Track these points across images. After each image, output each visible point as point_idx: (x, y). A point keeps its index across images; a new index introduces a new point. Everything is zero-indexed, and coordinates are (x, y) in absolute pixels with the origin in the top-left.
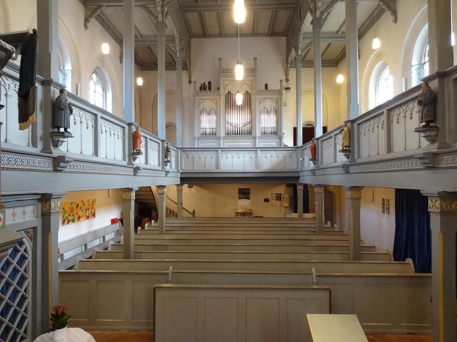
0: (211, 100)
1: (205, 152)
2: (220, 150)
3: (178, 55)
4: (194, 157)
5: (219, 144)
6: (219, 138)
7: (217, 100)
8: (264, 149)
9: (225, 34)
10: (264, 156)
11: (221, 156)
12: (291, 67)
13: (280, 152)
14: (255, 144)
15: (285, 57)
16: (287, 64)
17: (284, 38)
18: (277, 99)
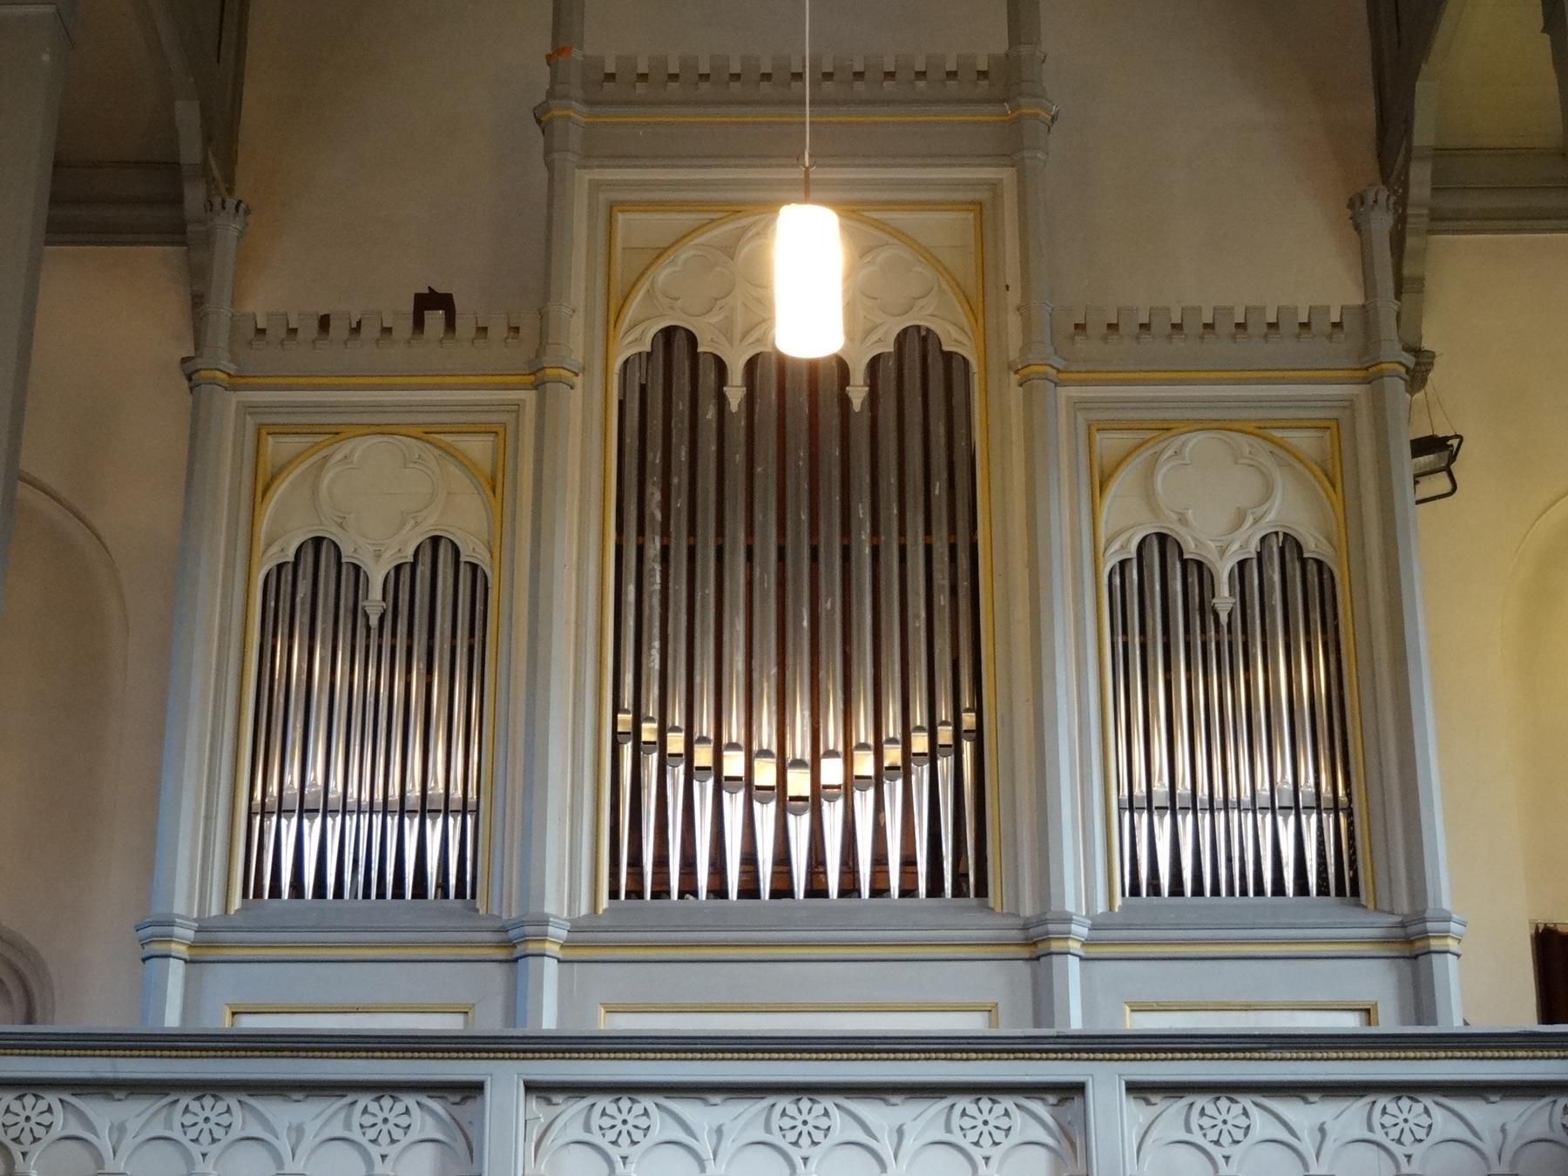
0: (427, 434)
1: (281, 1113)
2: (504, 1081)
5: (516, 999)
6: (514, 948)
13: (1441, 1118)
14: (1043, 999)
18: (1335, 426)
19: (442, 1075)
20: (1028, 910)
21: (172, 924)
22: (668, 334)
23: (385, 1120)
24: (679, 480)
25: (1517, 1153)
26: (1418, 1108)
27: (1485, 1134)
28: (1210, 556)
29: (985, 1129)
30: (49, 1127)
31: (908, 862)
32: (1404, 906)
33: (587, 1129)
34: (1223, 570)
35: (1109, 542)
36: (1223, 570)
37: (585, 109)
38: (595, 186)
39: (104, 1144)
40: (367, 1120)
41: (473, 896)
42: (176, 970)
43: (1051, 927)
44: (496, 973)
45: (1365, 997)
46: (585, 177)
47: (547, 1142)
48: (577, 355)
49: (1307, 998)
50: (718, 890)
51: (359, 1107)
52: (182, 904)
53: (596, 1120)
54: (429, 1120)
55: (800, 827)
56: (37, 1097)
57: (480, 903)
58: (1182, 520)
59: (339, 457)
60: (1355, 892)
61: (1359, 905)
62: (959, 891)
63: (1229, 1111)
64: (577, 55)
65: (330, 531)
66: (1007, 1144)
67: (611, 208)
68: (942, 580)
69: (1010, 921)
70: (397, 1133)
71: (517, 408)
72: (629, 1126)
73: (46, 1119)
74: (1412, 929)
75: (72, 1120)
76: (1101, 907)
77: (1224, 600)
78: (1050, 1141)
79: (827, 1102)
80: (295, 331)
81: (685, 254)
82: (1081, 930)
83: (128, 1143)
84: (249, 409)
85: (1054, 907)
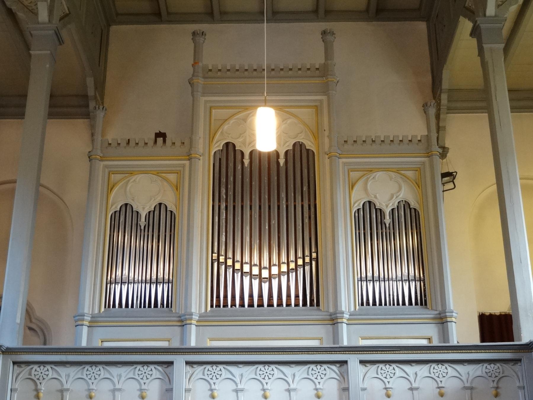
0: (158, 174)
1: (115, 371)
2: (179, 361)
3: (43, 15)
4: (62, 391)
5: (183, 337)
6: (183, 322)
7: (179, 173)
8: (375, 356)
9: (223, 13)
10: (378, 385)
11: (185, 384)
12: (450, 110)
13: (450, 370)
14: (336, 336)
15: (429, 78)
16: (439, 96)
17: (422, 26)
18: (419, 170)
19: (161, 359)
20: (331, 310)
21: (84, 316)
22: (227, 144)
23: (145, 373)
24: (231, 186)
25: (472, 380)
26: (444, 367)
27: (463, 375)
28: (384, 208)
29: (319, 374)
30: (47, 375)
31: (297, 296)
32: (440, 309)
33: (204, 374)
34: (387, 211)
35: (354, 203)
36: (387, 211)
37: (203, 79)
38: (206, 102)
39: (64, 380)
40: (140, 373)
41: (171, 307)
42: (85, 329)
43: (338, 315)
44: (178, 330)
45: (429, 335)
46: (203, 99)
47: (192, 378)
48: (201, 151)
49: (411, 335)
50: (242, 305)
51: (138, 369)
52: (87, 310)
53: (206, 372)
54: (158, 373)
55: (265, 287)
56: (44, 366)
57: (173, 309)
58: (376, 197)
59: (131, 181)
60: (426, 304)
61: (427, 308)
62: (312, 305)
63: (389, 368)
64: (200, 64)
65: (130, 202)
66: (325, 378)
67: (211, 108)
68: (306, 215)
69: (326, 313)
70: (149, 376)
71: (184, 166)
72: (216, 374)
73: (47, 373)
74: (442, 315)
75: (54, 373)
76: (352, 309)
77: (388, 220)
78: (338, 378)
79: (273, 366)
80: (119, 144)
81: (232, 121)
82: (346, 316)
83: (71, 379)
84: (106, 166)
85: (339, 309)
